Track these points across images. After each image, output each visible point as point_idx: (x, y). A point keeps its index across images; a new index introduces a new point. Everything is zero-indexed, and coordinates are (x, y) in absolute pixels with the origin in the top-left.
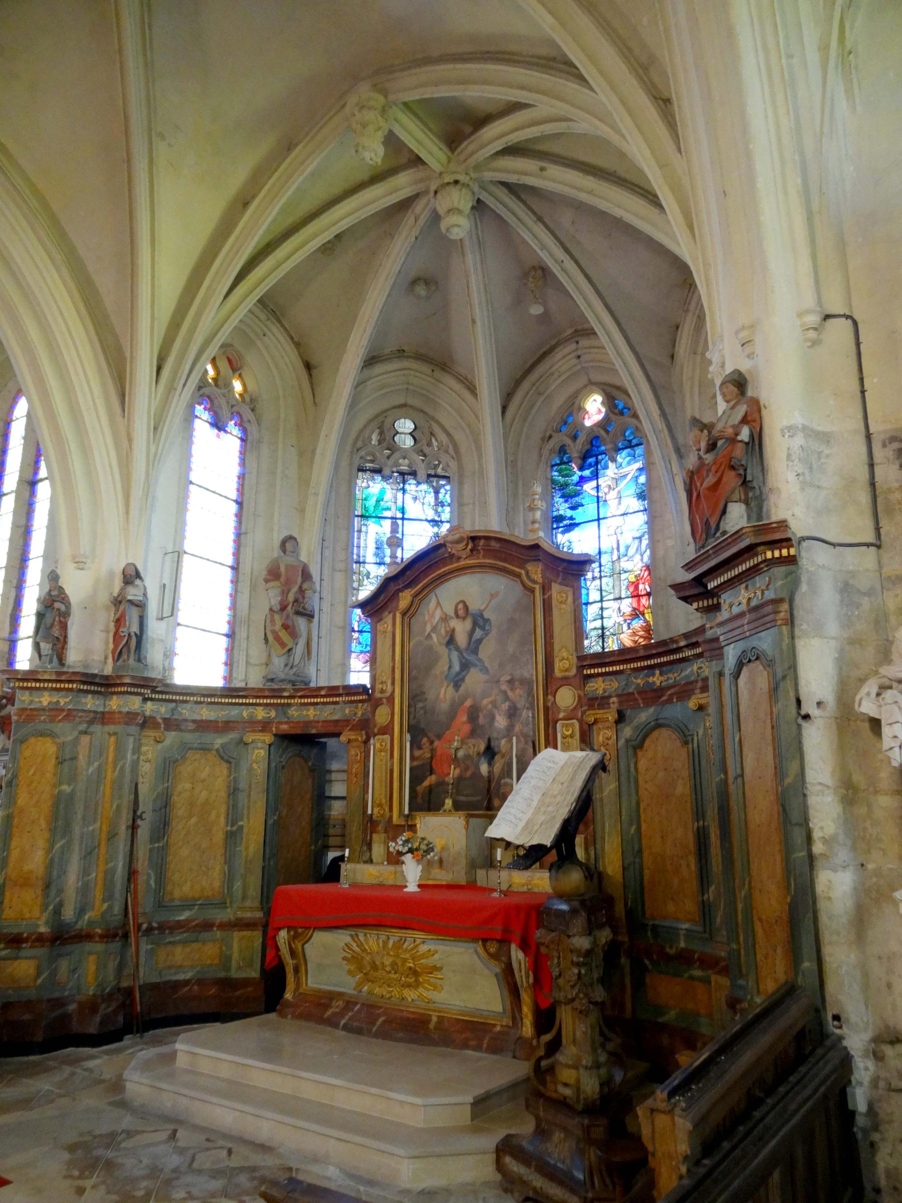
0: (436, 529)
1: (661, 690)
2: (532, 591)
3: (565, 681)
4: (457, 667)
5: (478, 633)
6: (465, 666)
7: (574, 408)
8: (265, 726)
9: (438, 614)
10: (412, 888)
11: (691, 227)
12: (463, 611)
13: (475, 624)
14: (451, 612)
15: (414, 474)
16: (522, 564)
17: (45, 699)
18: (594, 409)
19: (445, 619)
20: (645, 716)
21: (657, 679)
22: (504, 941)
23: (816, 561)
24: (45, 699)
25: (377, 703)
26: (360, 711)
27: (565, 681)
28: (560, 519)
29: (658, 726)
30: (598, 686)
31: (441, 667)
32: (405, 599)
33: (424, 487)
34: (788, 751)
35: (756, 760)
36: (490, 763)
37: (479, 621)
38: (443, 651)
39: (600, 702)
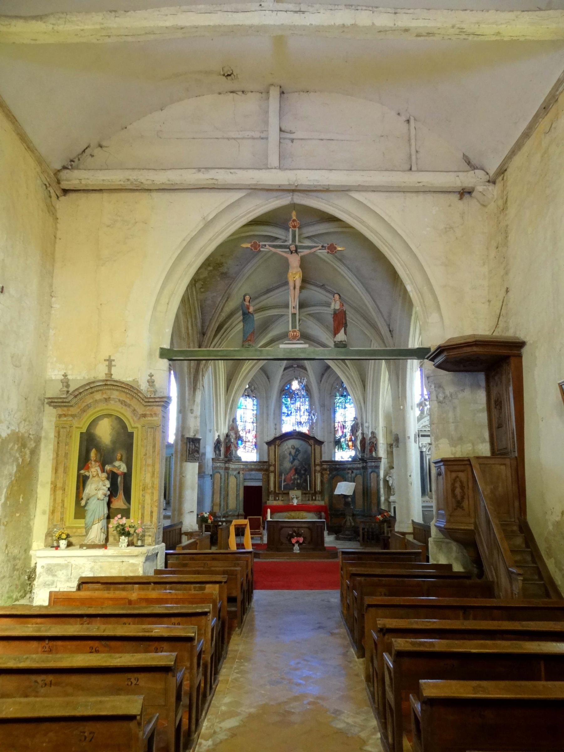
0: (253, 412)
1: (338, 468)
2: (311, 446)
3: (318, 465)
4: (292, 459)
5: (297, 453)
6: (294, 459)
7: (290, 383)
8: (243, 469)
9: (287, 447)
10: (295, 504)
11: (364, 403)
12: (293, 447)
13: (296, 451)
14: (290, 447)
15: (249, 396)
16: (309, 440)
17: (218, 464)
18: (295, 385)
19: (289, 448)
20: (334, 473)
21: (338, 466)
22: (320, 512)
23: (382, 460)
24: (218, 464)
25: (270, 465)
26: (265, 467)
27: (318, 465)
28: (284, 413)
29: (338, 475)
30: (325, 466)
31: (287, 459)
32: (278, 442)
33: (250, 399)
34: (378, 484)
35: (373, 484)
36: (300, 480)
37: (298, 450)
38: (288, 455)
39: (326, 470)
